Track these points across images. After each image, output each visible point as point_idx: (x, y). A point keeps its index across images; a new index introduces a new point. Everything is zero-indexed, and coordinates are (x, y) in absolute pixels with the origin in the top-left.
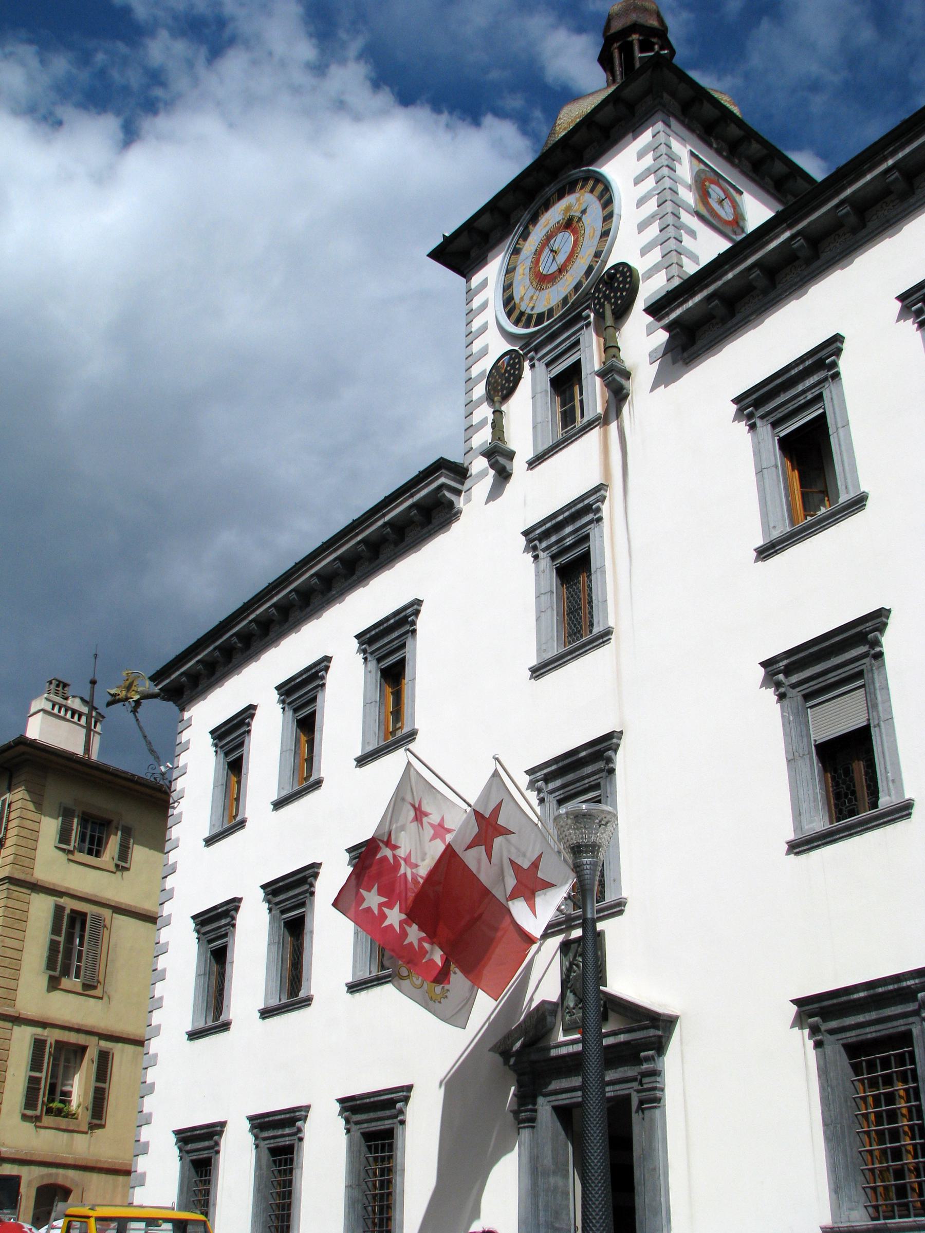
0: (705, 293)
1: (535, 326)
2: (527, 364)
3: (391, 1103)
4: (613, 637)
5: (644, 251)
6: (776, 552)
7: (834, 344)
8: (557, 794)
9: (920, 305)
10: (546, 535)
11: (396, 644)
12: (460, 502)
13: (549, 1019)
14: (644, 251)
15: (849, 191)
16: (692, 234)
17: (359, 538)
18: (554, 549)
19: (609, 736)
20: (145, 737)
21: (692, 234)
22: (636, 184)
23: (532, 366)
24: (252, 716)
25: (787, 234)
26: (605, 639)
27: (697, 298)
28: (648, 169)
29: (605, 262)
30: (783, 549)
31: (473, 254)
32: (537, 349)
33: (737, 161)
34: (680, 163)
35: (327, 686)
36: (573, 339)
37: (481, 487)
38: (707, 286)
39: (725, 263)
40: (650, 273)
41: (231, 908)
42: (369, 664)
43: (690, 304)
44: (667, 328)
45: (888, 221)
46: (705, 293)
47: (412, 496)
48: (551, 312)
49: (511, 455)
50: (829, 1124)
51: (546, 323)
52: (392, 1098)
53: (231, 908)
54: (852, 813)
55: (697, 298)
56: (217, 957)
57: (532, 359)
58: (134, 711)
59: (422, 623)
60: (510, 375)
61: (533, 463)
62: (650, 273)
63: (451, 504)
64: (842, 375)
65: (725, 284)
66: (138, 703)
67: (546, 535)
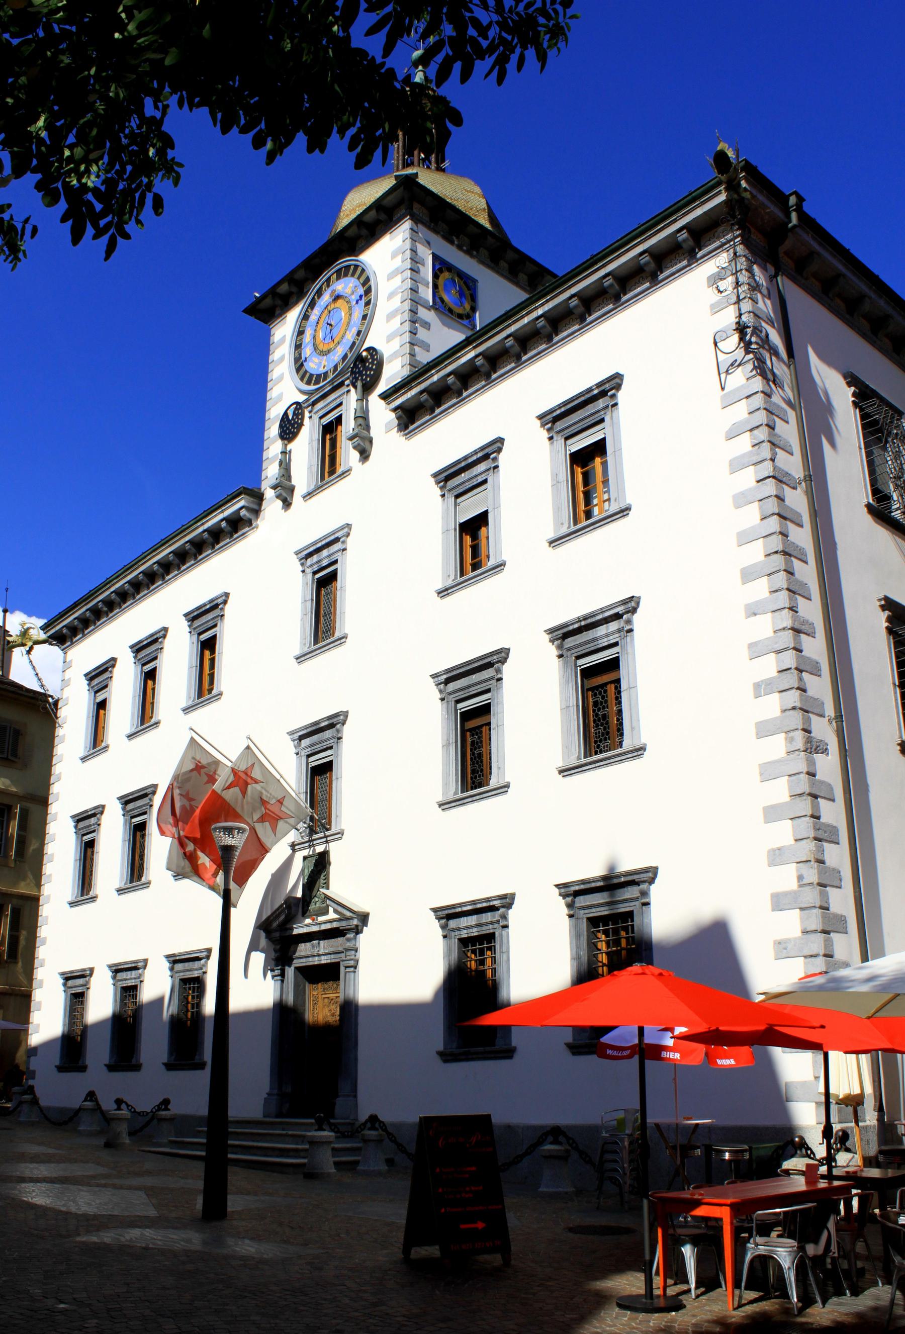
1: (315, 384)
2: (307, 414)
5: (390, 338)
7: (497, 445)
10: (310, 555)
11: (211, 624)
13: (293, 909)
14: (390, 338)
16: (427, 325)
20: (37, 675)
21: (427, 325)
22: (388, 279)
24: (113, 666)
25: (472, 354)
28: (397, 269)
31: (277, 312)
33: (475, 253)
34: (423, 265)
36: (338, 401)
37: (272, 505)
38: (420, 383)
41: (96, 813)
44: (394, 410)
47: (222, 512)
48: (326, 374)
49: (292, 490)
51: (322, 384)
53: (96, 813)
54: (481, 785)
56: (88, 848)
57: (310, 412)
58: (29, 652)
59: (229, 610)
60: (295, 423)
61: (308, 495)
62: (394, 356)
64: (500, 468)
65: (431, 384)
66: (31, 648)
67: (310, 555)
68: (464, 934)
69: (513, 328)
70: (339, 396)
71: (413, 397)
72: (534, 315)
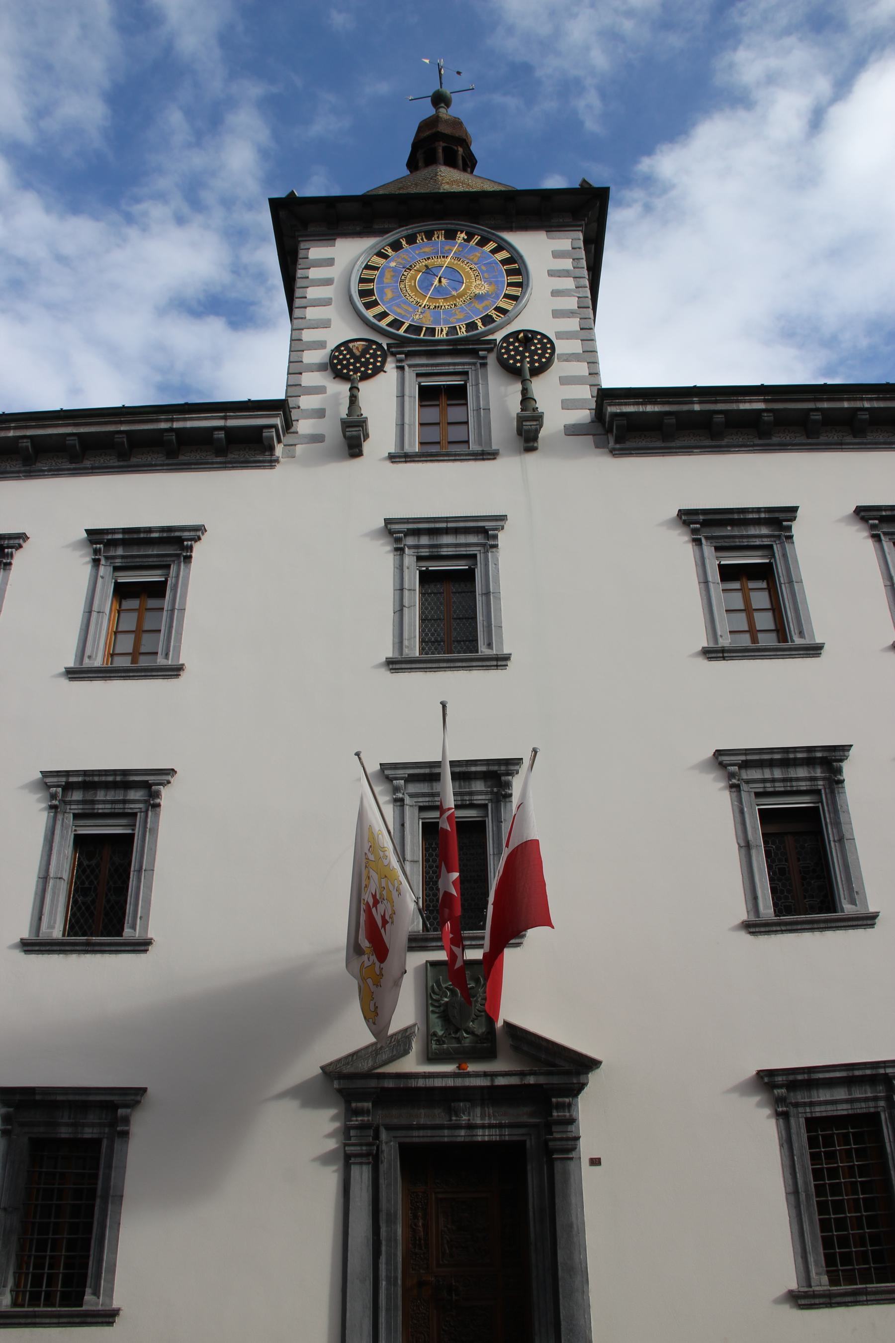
0: (666, 408)
3: (112, 1107)
4: (509, 663)
6: (724, 658)
8: (421, 799)
9: (877, 522)
12: (279, 450)
15: (825, 405)
17: (123, 428)
18: (425, 552)
19: (508, 762)
23: (401, 368)
25: (761, 406)
26: (500, 663)
27: (657, 408)
29: (509, 323)
30: (732, 658)
32: (409, 355)
35: (13, 567)
36: (459, 368)
39: (696, 395)
40: (569, 358)
42: (102, 569)
43: (649, 408)
45: (841, 444)
46: (666, 408)
50: (794, 1193)
52: (112, 1101)
55: (657, 408)
63: (272, 449)
68: (819, 1111)
69: (825, 405)
70: (469, 364)
71: (654, 413)
72: (858, 404)
